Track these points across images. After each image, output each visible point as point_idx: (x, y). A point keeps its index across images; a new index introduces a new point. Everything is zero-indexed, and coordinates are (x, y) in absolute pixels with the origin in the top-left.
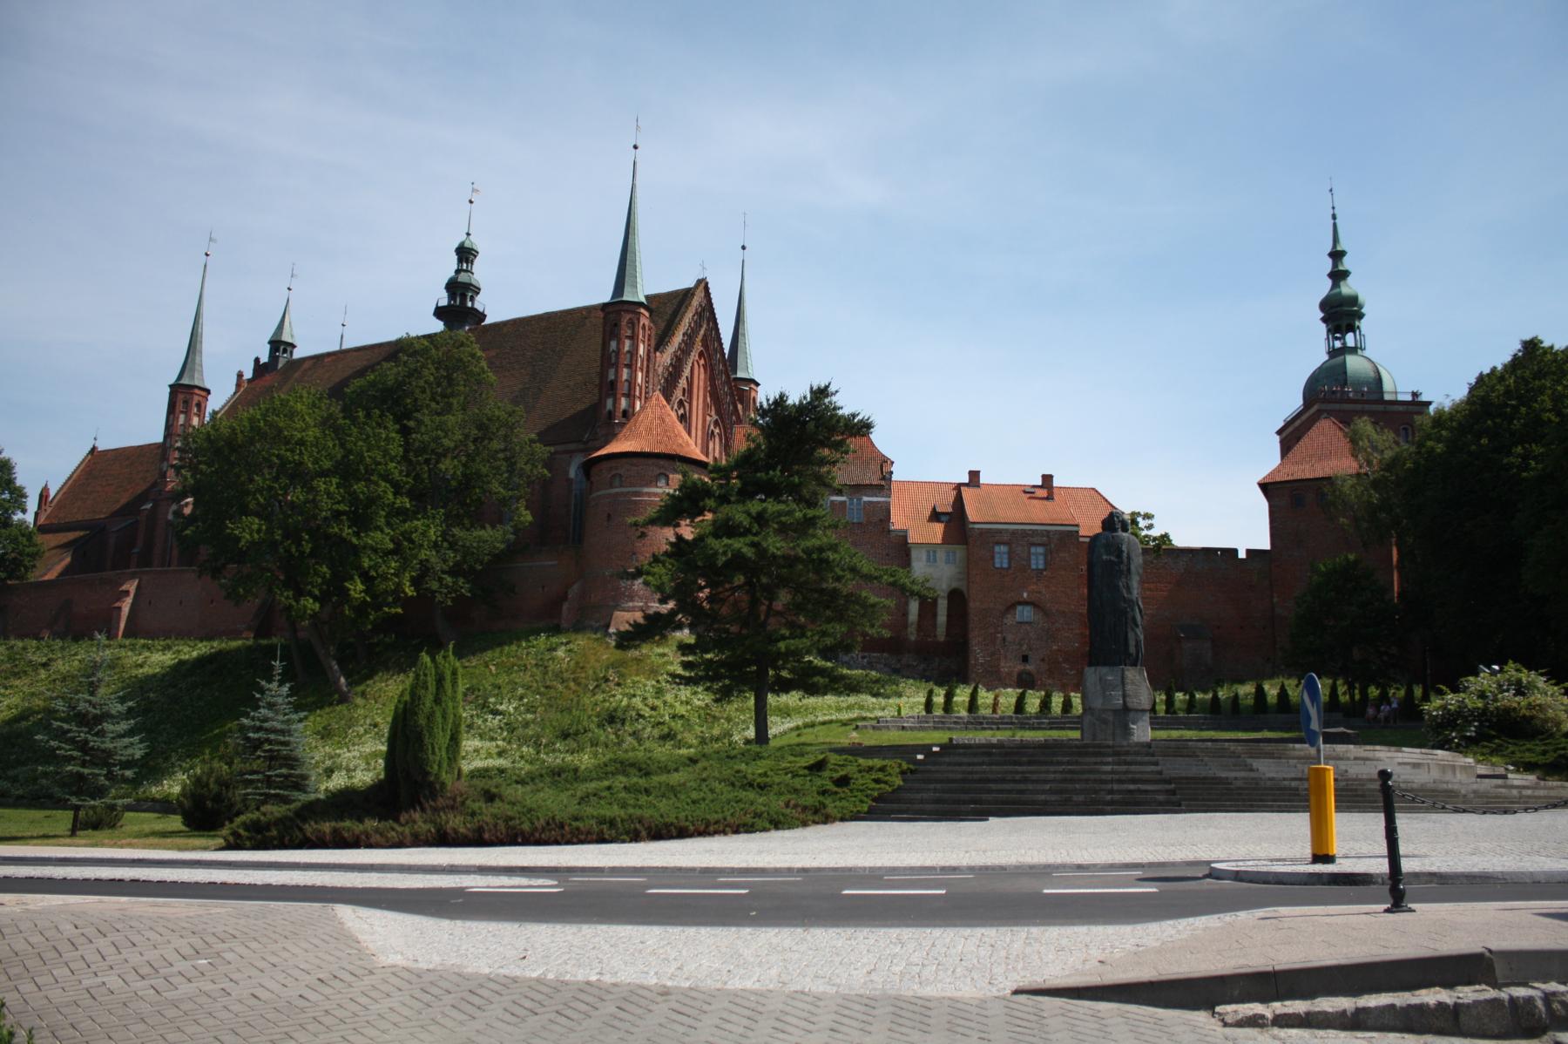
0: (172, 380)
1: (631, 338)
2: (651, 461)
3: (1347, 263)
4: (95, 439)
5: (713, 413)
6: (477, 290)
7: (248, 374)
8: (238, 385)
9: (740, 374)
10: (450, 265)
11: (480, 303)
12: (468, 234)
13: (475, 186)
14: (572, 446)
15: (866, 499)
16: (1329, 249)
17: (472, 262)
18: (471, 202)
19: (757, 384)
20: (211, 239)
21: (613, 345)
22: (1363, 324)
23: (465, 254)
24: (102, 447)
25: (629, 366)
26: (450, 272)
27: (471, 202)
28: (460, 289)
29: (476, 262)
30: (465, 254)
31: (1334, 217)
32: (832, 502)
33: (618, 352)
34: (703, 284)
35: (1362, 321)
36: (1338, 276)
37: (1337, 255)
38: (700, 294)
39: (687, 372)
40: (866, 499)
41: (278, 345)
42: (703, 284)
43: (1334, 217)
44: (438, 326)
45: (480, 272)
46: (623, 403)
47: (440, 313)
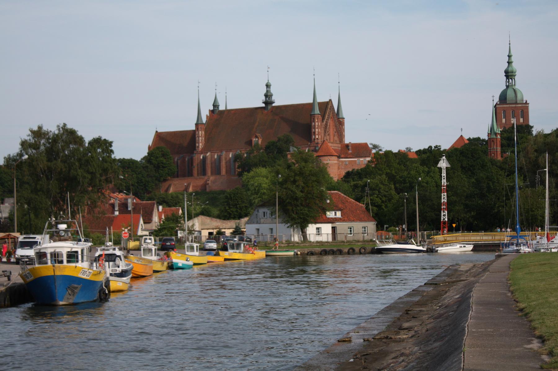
0: (195, 122)
1: (318, 122)
2: (326, 157)
3: (513, 59)
4: (156, 128)
5: (335, 130)
6: (272, 95)
7: (208, 115)
8: (207, 118)
9: (340, 117)
10: (264, 91)
11: (273, 98)
12: (268, 80)
13: (269, 70)
14: (306, 146)
15: (367, 159)
16: (508, 54)
17: (270, 88)
18: (268, 71)
19: (344, 118)
20: (199, 83)
21: (313, 124)
22: (516, 78)
23: (268, 86)
24: (159, 131)
25: (318, 128)
26: (265, 92)
27: (268, 71)
28: (268, 95)
29: (271, 87)
30: (268, 86)
31: (510, 44)
32: (361, 160)
33: (315, 125)
34: (330, 100)
35: (516, 77)
36: (509, 63)
37: (509, 56)
38: (330, 103)
39: (329, 124)
40: (367, 159)
41: (215, 105)
42: (330, 100)
43: (510, 44)
44: (264, 105)
45: (273, 90)
46: (317, 137)
47: (263, 103)
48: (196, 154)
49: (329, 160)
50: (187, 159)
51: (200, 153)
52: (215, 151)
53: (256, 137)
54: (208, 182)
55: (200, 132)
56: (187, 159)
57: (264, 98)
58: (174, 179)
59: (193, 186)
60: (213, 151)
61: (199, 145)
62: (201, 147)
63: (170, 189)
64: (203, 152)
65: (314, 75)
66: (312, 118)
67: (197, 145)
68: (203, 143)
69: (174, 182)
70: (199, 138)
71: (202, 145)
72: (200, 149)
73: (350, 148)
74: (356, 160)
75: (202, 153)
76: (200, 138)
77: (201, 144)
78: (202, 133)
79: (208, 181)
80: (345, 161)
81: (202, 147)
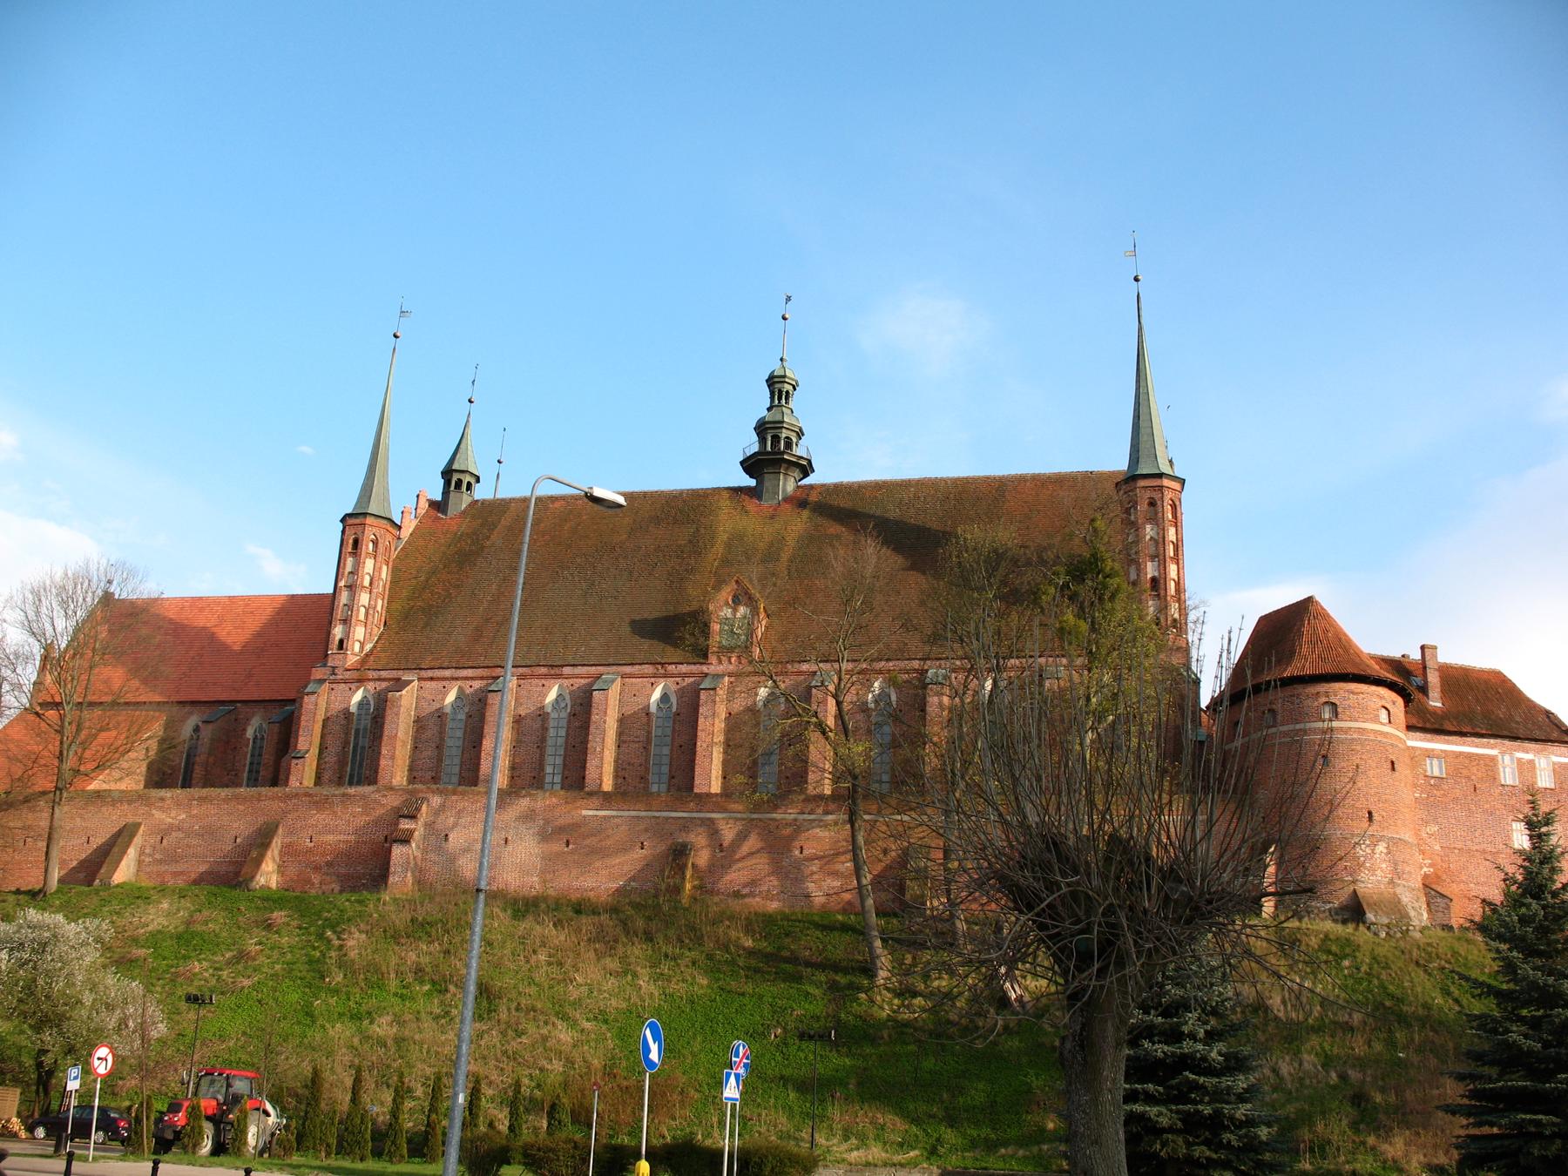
18: (784, 318)
23: (778, 387)
27: (784, 318)
30: (778, 387)
45: (800, 410)
48: (321, 681)
49: (1384, 714)
50: (250, 733)
51: (345, 682)
52: (447, 673)
53: (742, 597)
54: (405, 825)
55: (369, 565)
56: (250, 733)
57: (750, 443)
58: (166, 793)
59: (288, 851)
60: (438, 673)
61: (347, 634)
62: (357, 647)
63: (124, 852)
64: (371, 674)
65: (1136, 279)
66: (1143, 498)
67: (338, 631)
68: (377, 632)
69: (157, 814)
70: (352, 597)
71: (369, 634)
72: (352, 660)
73: (1433, 678)
74: (1493, 759)
75: (361, 681)
76: (364, 598)
77: (359, 632)
78: (377, 569)
79: (413, 817)
80: (1429, 754)
81: (368, 647)
